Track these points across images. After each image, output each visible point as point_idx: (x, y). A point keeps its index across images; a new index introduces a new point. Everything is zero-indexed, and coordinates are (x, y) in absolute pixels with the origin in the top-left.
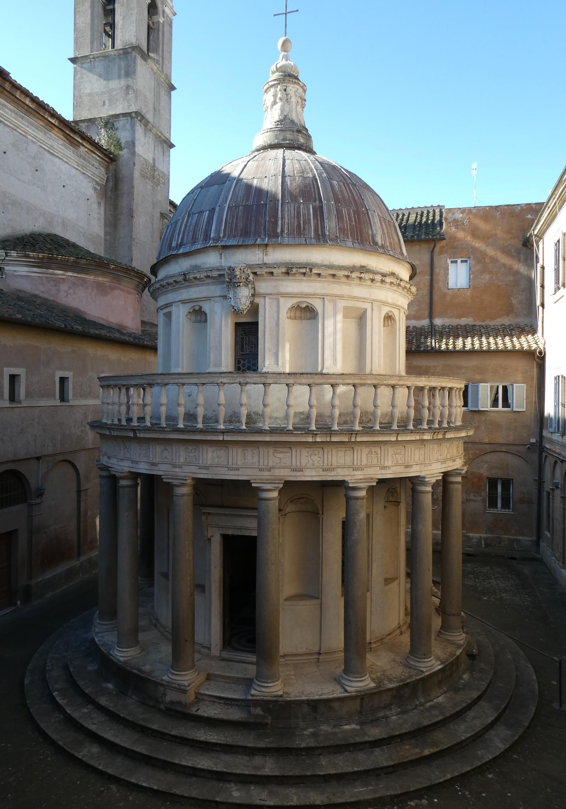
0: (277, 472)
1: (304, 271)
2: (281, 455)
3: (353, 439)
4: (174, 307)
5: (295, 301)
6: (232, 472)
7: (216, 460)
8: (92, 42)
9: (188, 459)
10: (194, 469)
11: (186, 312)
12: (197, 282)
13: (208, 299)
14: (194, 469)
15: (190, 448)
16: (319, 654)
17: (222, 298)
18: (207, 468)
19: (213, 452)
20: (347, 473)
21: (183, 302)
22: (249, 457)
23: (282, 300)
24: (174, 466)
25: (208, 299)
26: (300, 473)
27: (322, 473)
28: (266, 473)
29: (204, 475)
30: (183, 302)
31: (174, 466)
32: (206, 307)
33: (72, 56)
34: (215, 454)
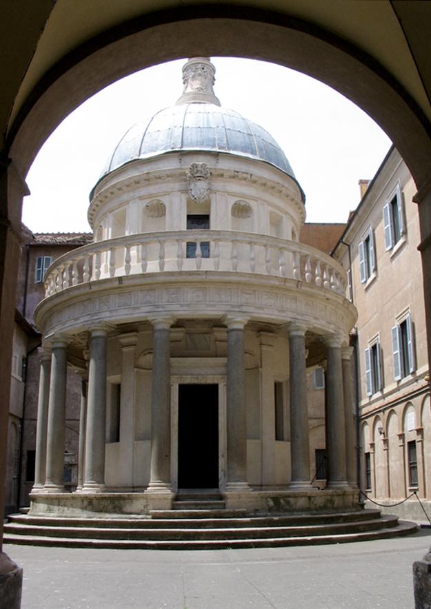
1: (245, 176)
2: (247, 296)
4: (130, 203)
5: (238, 199)
6: (209, 308)
9: (170, 300)
11: (144, 205)
16: (261, 486)
17: (180, 193)
18: (189, 305)
19: (193, 293)
20: (292, 316)
21: (141, 198)
22: (223, 297)
26: (261, 311)
27: (277, 313)
32: (165, 200)
34: (194, 295)
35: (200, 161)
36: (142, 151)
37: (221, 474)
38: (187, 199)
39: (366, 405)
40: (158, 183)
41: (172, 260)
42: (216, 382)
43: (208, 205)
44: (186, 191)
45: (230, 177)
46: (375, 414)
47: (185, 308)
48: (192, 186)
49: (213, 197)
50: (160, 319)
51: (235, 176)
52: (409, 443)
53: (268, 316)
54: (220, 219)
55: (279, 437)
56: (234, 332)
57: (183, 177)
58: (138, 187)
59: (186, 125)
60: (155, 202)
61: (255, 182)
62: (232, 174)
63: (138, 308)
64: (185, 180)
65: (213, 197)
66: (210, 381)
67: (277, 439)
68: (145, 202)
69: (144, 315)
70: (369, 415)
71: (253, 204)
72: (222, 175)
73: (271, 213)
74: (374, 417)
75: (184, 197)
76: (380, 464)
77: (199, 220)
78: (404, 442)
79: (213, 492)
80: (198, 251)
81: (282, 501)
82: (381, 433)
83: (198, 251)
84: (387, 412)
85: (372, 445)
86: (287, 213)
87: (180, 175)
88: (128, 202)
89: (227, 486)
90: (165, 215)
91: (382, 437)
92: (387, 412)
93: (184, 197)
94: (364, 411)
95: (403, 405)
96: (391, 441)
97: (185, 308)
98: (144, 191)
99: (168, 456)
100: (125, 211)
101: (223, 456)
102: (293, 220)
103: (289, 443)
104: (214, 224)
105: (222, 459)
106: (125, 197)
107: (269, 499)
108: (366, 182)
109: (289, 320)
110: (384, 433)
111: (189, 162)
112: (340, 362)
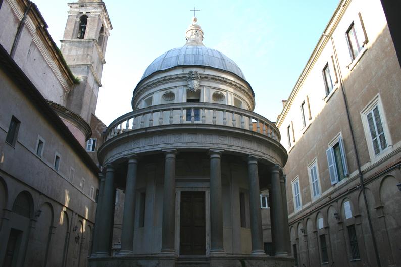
0: (220, 146)
2: (222, 139)
3: (253, 135)
7: (191, 140)
8: (73, 36)
10: (179, 145)
12: (171, 81)
13: (176, 87)
14: (179, 145)
15: (177, 135)
18: (186, 143)
21: (161, 90)
22: (207, 139)
23: (211, 90)
24: (168, 144)
25: (176, 87)
26: (230, 148)
28: (216, 146)
29: (184, 147)
30: (161, 90)
31: (168, 144)
32: (174, 91)
33: (62, 39)
34: (190, 138)
35: (194, 70)
36: (162, 67)
37: (207, 246)
38: (187, 90)
39: (292, 217)
40: (170, 82)
41: (179, 117)
42: (204, 190)
43: (198, 93)
44: (186, 86)
45: (212, 79)
46: (298, 221)
47: (185, 145)
48: (190, 83)
49: (201, 89)
50: (169, 151)
51: (214, 79)
52: (321, 236)
53: (235, 151)
54: (206, 97)
55: (243, 224)
56: (215, 159)
57: (184, 78)
58: (159, 85)
59: (187, 53)
60: (168, 92)
61: (225, 82)
62: (213, 77)
63: (156, 145)
64: (186, 80)
65: (201, 89)
66: (200, 190)
67: (241, 226)
68: (163, 93)
69: (160, 149)
70: (293, 223)
71: (224, 93)
72: (206, 78)
73: (235, 99)
74: (297, 223)
75: (185, 89)
76: (303, 250)
77: (194, 97)
78: (317, 235)
79: (202, 257)
80: (193, 114)
81: (246, 262)
82: (302, 232)
83: (193, 114)
84: (306, 219)
85: (297, 239)
86: (244, 100)
87: (183, 77)
88: (153, 93)
89: (211, 252)
90: (174, 99)
91: (303, 234)
92: (306, 219)
93: (185, 89)
94: (289, 221)
95: (315, 214)
96: (309, 236)
97: (185, 145)
98: (162, 87)
99: (173, 233)
100: (152, 97)
101: (208, 235)
102: (248, 105)
103: (250, 229)
104: (201, 101)
105: (208, 237)
106: (152, 91)
107: (238, 261)
108: (286, 101)
109: (247, 153)
110: (304, 231)
111: (187, 71)
112: (279, 184)
